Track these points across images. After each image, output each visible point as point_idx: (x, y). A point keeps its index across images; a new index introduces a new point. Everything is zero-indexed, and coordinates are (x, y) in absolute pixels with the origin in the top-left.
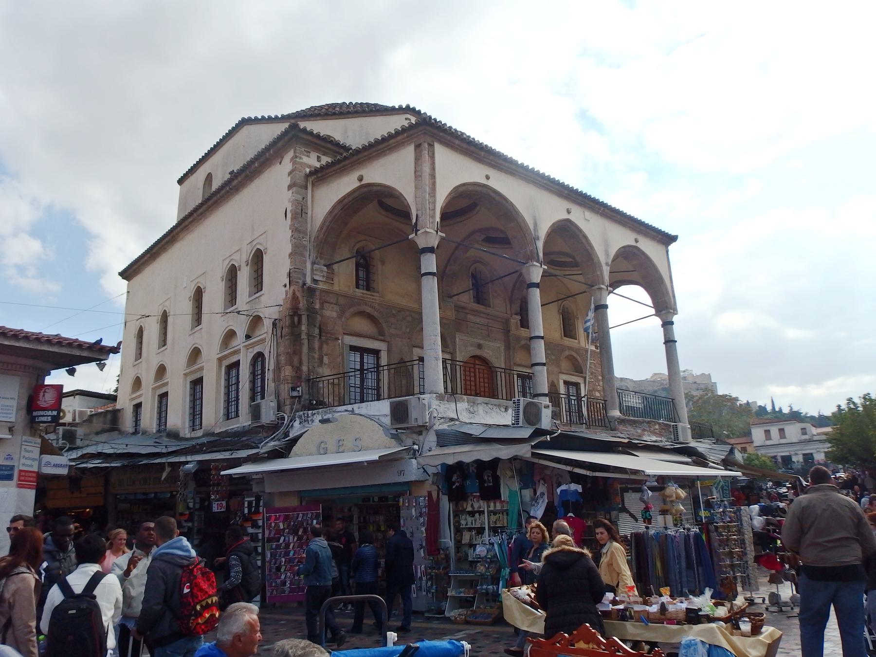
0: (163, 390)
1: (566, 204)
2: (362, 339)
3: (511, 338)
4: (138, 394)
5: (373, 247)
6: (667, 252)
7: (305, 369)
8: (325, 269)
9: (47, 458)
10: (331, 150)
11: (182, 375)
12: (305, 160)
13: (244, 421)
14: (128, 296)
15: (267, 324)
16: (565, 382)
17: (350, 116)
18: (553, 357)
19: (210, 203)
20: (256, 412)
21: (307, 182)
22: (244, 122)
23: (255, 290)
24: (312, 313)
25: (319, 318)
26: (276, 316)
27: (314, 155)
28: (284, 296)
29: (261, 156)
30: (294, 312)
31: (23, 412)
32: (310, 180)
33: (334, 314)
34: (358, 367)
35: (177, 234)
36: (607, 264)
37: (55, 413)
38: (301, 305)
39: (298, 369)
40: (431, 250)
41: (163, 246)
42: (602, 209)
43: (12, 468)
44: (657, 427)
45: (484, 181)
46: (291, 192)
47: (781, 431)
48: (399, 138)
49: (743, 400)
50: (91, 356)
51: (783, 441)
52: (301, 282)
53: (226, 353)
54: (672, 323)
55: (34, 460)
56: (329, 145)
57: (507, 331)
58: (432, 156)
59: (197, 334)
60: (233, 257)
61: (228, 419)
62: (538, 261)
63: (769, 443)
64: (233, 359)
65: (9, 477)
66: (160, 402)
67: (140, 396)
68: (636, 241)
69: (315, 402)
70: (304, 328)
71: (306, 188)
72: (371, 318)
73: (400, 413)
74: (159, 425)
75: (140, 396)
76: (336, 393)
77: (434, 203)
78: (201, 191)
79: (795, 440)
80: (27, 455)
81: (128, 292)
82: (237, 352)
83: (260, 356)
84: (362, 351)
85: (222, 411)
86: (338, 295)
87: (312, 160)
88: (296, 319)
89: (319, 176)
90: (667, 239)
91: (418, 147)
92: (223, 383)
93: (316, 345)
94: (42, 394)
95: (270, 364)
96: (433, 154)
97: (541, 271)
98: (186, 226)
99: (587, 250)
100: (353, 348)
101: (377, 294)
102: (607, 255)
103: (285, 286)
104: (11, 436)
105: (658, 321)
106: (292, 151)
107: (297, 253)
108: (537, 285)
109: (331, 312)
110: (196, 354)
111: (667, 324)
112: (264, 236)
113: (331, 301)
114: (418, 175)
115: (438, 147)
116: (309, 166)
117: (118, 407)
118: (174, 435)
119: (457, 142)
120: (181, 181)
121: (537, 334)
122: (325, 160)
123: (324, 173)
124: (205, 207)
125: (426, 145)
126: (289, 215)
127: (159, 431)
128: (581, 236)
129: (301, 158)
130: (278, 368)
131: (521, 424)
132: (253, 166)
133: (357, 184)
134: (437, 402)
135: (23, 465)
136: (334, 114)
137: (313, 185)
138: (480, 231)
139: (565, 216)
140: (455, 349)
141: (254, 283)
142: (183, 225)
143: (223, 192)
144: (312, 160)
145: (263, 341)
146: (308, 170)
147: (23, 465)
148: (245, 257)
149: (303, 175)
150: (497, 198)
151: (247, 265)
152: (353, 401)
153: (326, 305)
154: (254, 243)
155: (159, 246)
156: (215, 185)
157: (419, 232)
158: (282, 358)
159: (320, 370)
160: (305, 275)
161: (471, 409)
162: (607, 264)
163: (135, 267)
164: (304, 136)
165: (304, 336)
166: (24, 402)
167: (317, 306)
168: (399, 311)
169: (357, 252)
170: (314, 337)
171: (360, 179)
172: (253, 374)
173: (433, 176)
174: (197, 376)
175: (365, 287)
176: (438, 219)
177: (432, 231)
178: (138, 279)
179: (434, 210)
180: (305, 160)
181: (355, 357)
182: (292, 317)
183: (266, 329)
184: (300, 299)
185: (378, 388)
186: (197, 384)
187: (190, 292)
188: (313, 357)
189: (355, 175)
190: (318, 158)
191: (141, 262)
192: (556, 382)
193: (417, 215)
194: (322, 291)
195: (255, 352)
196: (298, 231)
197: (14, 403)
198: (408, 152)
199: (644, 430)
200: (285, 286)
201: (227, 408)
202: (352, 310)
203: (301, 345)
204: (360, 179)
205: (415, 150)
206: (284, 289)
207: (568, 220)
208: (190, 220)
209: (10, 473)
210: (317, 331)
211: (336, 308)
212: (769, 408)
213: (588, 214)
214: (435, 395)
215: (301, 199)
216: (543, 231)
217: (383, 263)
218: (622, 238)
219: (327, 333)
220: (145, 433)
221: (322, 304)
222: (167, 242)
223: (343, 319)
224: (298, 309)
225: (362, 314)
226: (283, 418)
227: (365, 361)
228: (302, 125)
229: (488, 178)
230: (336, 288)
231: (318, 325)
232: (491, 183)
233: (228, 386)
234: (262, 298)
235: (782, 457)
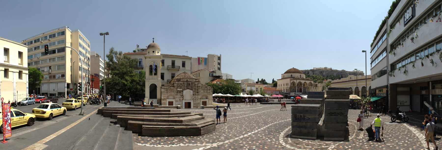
13: (287, 92)
30: (290, 88)
73: (295, 93)
89: (291, 80)
95: (289, 89)
107: (290, 84)
109: (292, 87)
118: (283, 92)
183: (289, 88)
186: (284, 89)
196: (290, 83)
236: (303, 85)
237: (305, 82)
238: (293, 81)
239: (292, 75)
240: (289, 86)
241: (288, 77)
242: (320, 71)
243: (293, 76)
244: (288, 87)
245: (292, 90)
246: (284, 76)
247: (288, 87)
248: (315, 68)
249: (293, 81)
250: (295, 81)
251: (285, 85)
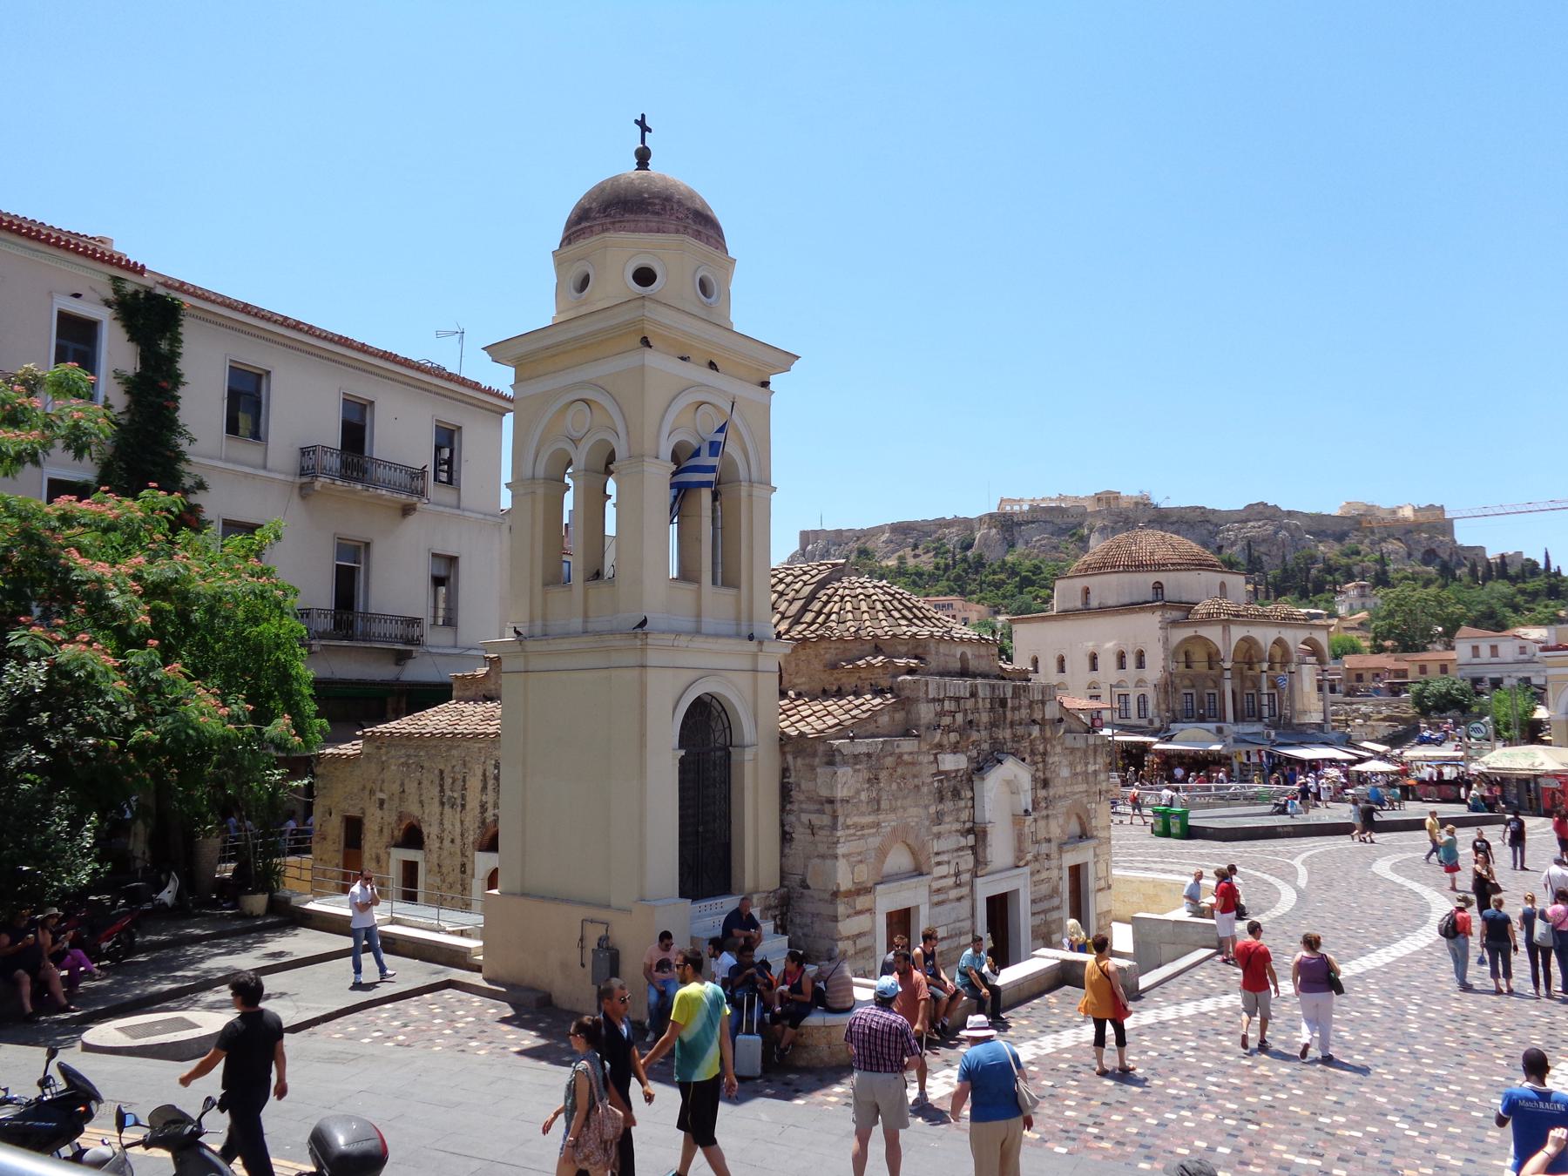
12: (1167, 616)
24: (1172, 682)
30: (1166, 684)
39: (1168, 705)
47: (1494, 649)
49: (1492, 554)
57: (1242, 673)
63: (1476, 660)
72: (1191, 680)
79: (1510, 659)
89: (1175, 623)
109: (1177, 681)
114: (1224, 639)
130: (1158, 704)
158: (1161, 701)
172: (1139, 702)
196: (1166, 649)
212: (1542, 566)
235: (1491, 679)
236: (1265, 666)
237: (1279, 642)
238: (1188, 632)
239: (1158, 587)
240: (1154, 671)
241: (1127, 600)
242: (1058, 521)
243: (1169, 594)
244: (1140, 683)
245: (1178, 707)
246: (1087, 591)
247: (1140, 683)
248: (1012, 501)
249: (1188, 632)
250: (1213, 634)
251: (1107, 662)
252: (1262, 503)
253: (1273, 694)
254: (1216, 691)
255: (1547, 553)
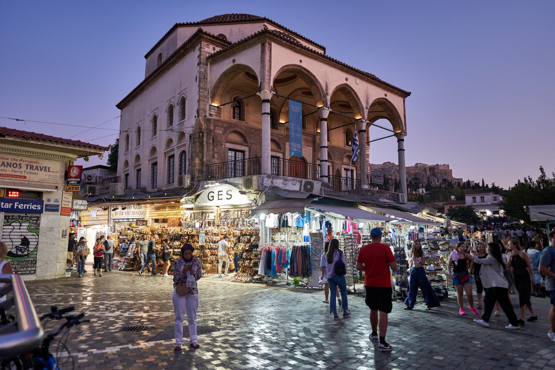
0: (139, 168)
1: (345, 75)
2: (235, 145)
3: (316, 146)
4: (127, 169)
5: (243, 97)
6: (404, 101)
7: (205, 160)
8: (216, 108)
9: (75, 202)
10: (220, 44)
11: (148, 161)
12: (206, 49)
13: (176, 184)
14: (121, 118)
15: (187, 136)
16: (345, 169)
17: (233, 23)
18: (339, 156)
19: (159, 71)
20: (181, 181)
21: (207, 62)
22: (177, 26)
23: (182, 118)
24: (209, 131)
25: (213, 134)
26: (191, 133)
27: (211, 46)
28: (195, 123)
29: (184, 46)
31: (63, 179)
32: (210, 60)
33: (221, 132)
34: (233, 159)
35: (144, 86)
36: (367, 108)
37: (79, 180)
38: (203, 127)
39: (202, 160)
40: (267, 101)
41: (137, 92)
42: (367, 78)
43: (58, 206)
44: (388, 195)
45: (299, 64)
46: (199, 67)
47: (482, 198)
48: (253, 40)
49: (465, 181)
50: (95, 152)
51: (483, 204)
52: (203, 115)
53: (168, 150)
54: (403, 140)
55: (69, 202)
56: (219, 41)
58: (270, 50)
59: (154, 140)
60: (172, 100)
61: (169, 183)
62: (326, 107)
64: (172, 153)
65: (57, 210)
66: (138, 174)
67: (128, 170)
68: (386, 95)
69: (209, 177)
70: (205, 139)
71: (207, 65)
74: (137, 185)
75: (128, 170)
76: (222, 173)
77: (270, 76)
78: (156, 63)
79: (489, 203)
80: (66, 200)
81: (121, 116)
82: (173, 150)
83: (184, 152)
84: (236, 151)
85: (166, 180)
86: (223, 122)
87: (209, 49)
88: (201, 134)
89: (214, 59)
90: (405, 94)
91: (263, 45)
92: (167, 165)
93: (211, 148)
94: (72, 170)
96: (271, 49)
97: (328, 112)
98: (148, 82)
99: (356, 101)
100: (230, 149)
101: (244, 122)
102: (367, 102)
103: (196, 117)
104: (56, 190)
105: (395, 139)
106: (200, 44)
108: (325, 120)
109: (219, 131)
110: (154, 150)
111: (400, 141)
112: (186, 90)
113: (219, 125)
114: (263, 60)
115: (274, 46)
116: (209, 53)
117: (117, 175)
118: (144, 191)
119: (284, 42)
120: (146, 57)
121: (324, 145)
122: (218, 49)
123: (216, 58)
124: (157, 72)
125: (267, 44)
126: (198, 80)
127: (137, 188)
128: (353, 93)
129: (204, 49)
131: (302, 191)
132: (180, 52)
133: (231, 64)
134: (267, 179)
135: (64, 204)
136: (225, 22)
137: (211, 64)
138: (299, 89)
139: (345, 82)
140: (285, 151)
141: (181, 115)
142: (147, 81)
143: (166, 65)
144: (209, 49)
145: (185, 145)
146: (208, 55)
147: (64, 204)
148: (176, 102)
149: (205, 57)
150: (306, 72)
151: (178, 105)
152: (230, 176)
153: (217, 127)
154: (181, 93)
155: (136, 92)
156: (164, 59)
157: (261, 91)
159: (213, 160)
160: (206, 112)
161: (285, 183)
162: (367, 108)
163: (124, 102)
164: (205, 36)
165: (205, 143)
166: (63, 174)
167: (212, 128)
168: (255, 131)
169: (234, 99)
170: (210, 144)
171: (234, 61)
172: (181, 161)
173: (270, 61)
174: (154, 161)
175: (238, 118)
176: (272, 84)
177: (268, 91)
178: (126, 109)
179: (270, 79)
180: (206, 49)
181: (232, 154)
182: (199, 133)
184: (203, 124)
185: (243, 170)
187: (151, 117)
188: (210, 154)
189: (231, 59)
190: (214, 48)
191: (127, 100)
192: (340, 169)
193: (261, 82)
194: (214, 120)
195: (182, 150)
197: (58, 174)
198: (258, 48)
199: (380, 196)
200: (196, 117)
201: (169, 178)
202: (230, 130)
203: (203, 148)
204: (234, 61)
205: (262, 46)
206: (195, 119)
207: (347, 84)
208: (150, 79)
209: (57, 208)
210: (211, 141)
211: (222, 129)
212: (481, 185)
213: (359, 81)
214: (265, 175)
215: (204, 71)
216: (331, 91)
217: (247, 105)
218: (377, 93)
219: (217, 142)
220: (130, 188)
221: (215, 126)
222: (140, 90)
223: (226, 135)
224: (202, 129)
225: (236, 132)
226: (194, 185)
227: (237, 156)
228: (205, 29)
229: (301, 61)
230: (222, 118)
231: (212, 137)
232: (302, 64)
233: (169, 167)
234: (185, 123)
238: (226, 65)
240: (190, 123)
249: (226, 65)
252: (389, 162)
253: (352, 171)
254: (280, 155)
255: (483, 180)
